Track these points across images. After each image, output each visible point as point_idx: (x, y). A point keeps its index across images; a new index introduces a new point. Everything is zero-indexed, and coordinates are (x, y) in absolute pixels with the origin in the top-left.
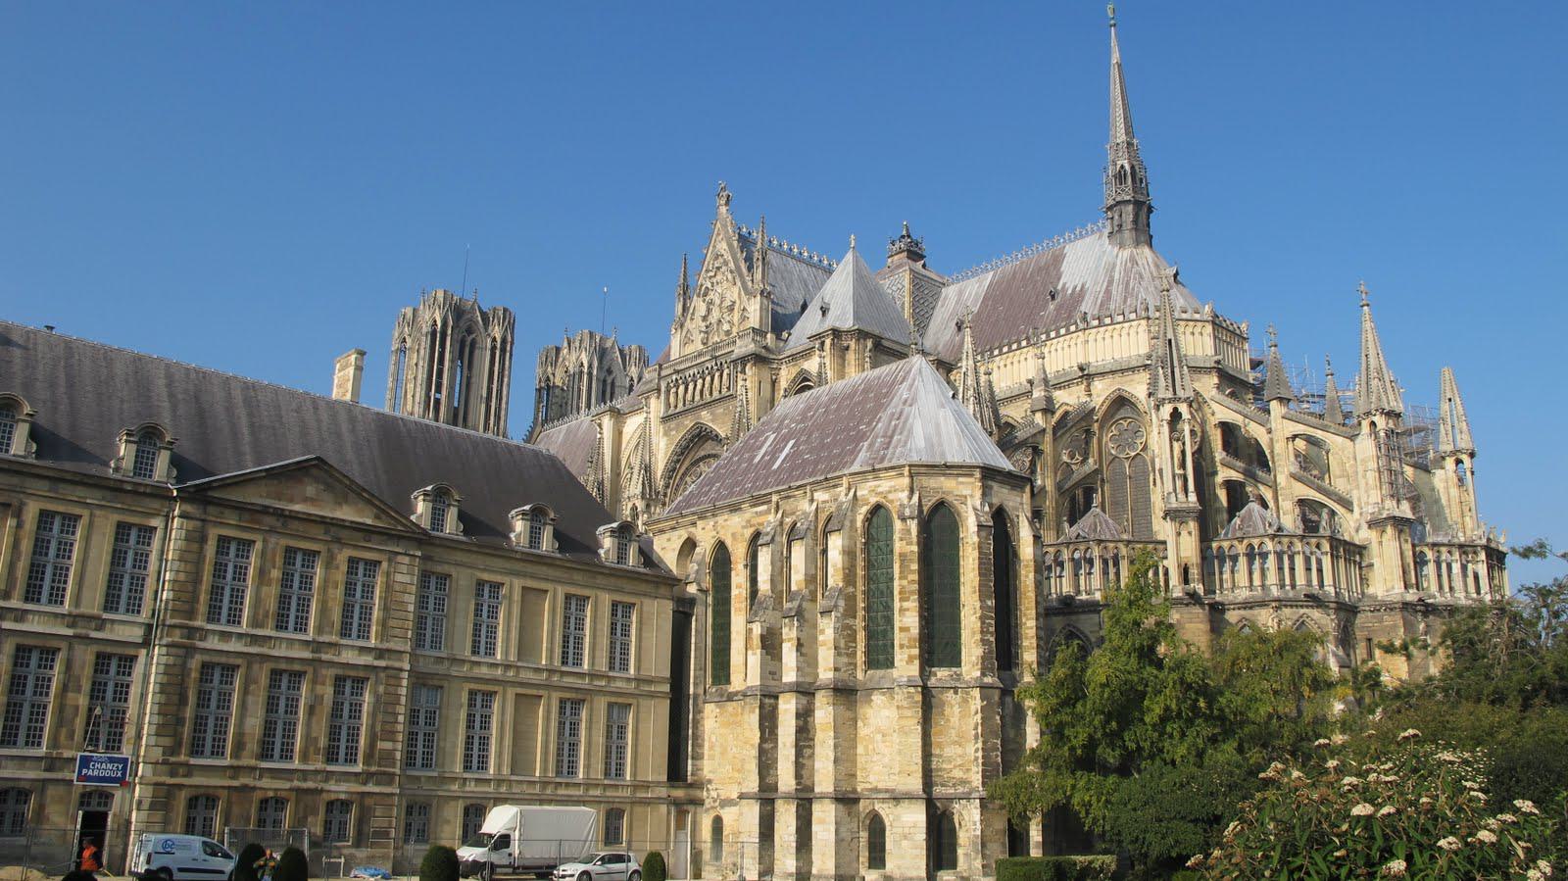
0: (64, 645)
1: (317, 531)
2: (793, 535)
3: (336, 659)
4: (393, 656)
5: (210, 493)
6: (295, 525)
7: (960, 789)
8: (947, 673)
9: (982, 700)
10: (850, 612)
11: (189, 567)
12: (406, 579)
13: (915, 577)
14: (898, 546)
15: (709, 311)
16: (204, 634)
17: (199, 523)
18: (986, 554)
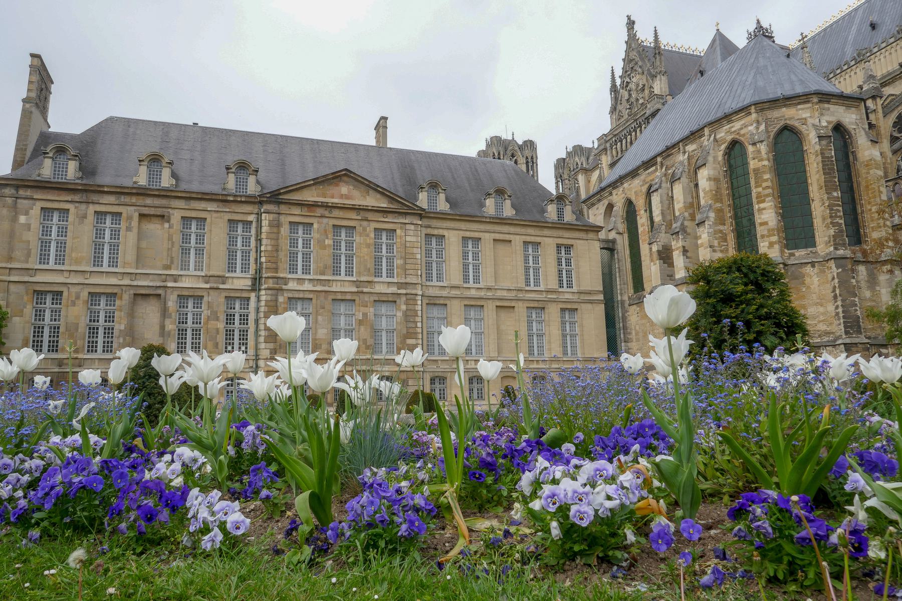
0: (205, 294)
1: (353, 215)
2: (673, 180)
3: (372, 290)
4: (411, 286)
5: (281, 197)
6: (336, 213)
7: (826, 339)
8: (803, 253)
9: (837, 268)
10: (721, 220)
11: (273, 242)
12: (413, 239)
13: (769, 184)
14: (753, 164)
15: (630, 95)
16: (286, 281)
17: (276, 216)
18: (828, 157)
